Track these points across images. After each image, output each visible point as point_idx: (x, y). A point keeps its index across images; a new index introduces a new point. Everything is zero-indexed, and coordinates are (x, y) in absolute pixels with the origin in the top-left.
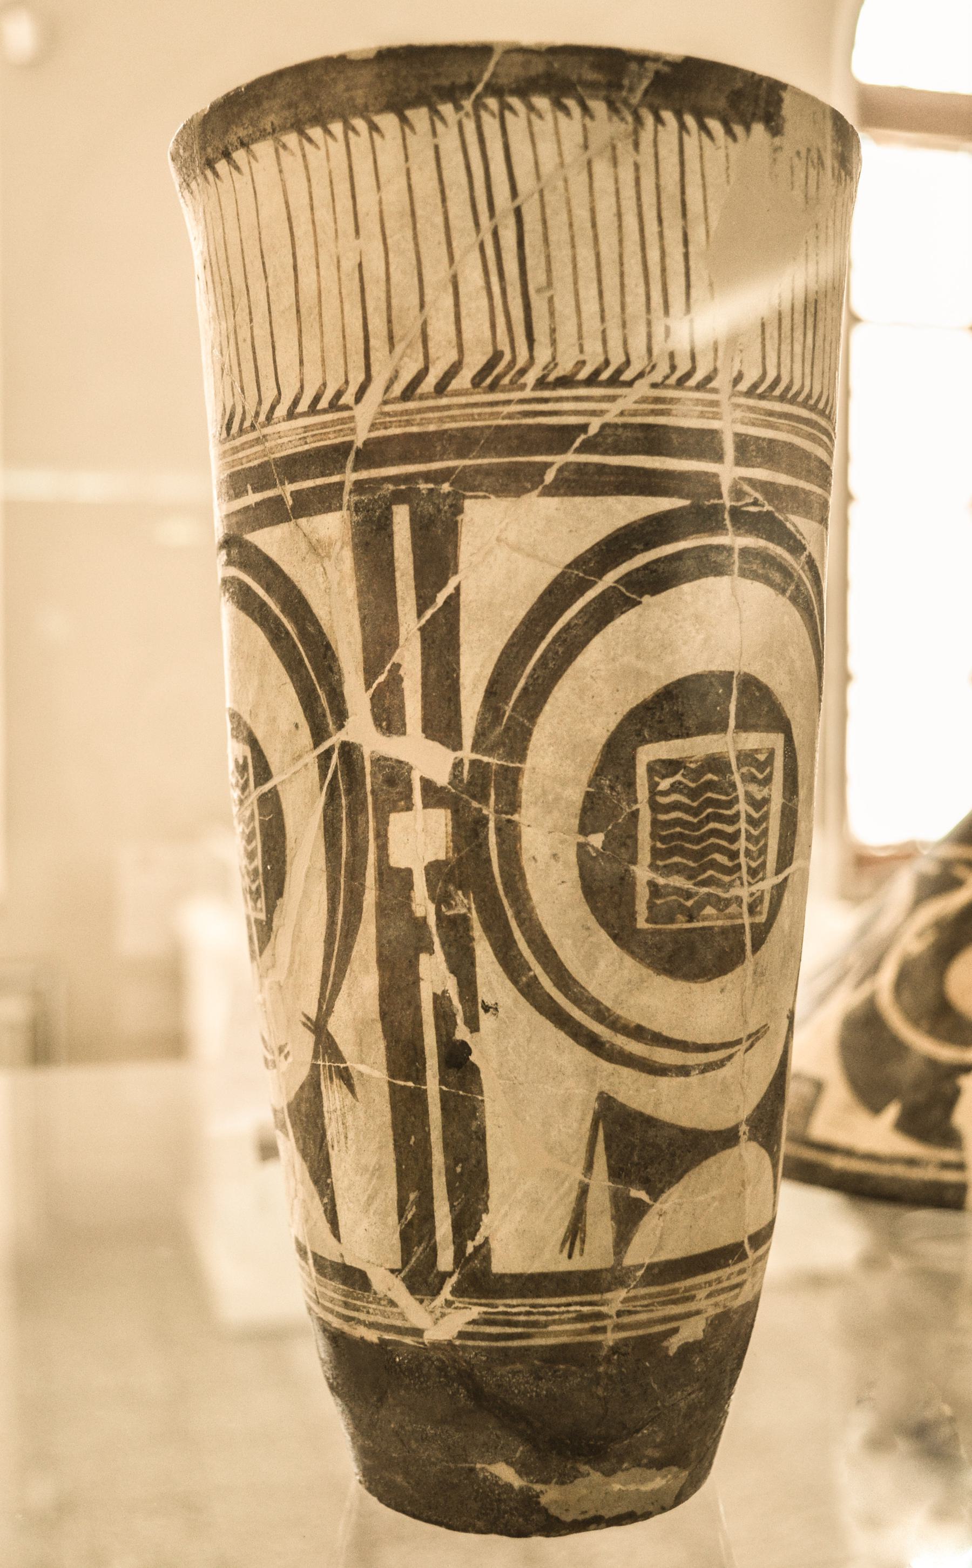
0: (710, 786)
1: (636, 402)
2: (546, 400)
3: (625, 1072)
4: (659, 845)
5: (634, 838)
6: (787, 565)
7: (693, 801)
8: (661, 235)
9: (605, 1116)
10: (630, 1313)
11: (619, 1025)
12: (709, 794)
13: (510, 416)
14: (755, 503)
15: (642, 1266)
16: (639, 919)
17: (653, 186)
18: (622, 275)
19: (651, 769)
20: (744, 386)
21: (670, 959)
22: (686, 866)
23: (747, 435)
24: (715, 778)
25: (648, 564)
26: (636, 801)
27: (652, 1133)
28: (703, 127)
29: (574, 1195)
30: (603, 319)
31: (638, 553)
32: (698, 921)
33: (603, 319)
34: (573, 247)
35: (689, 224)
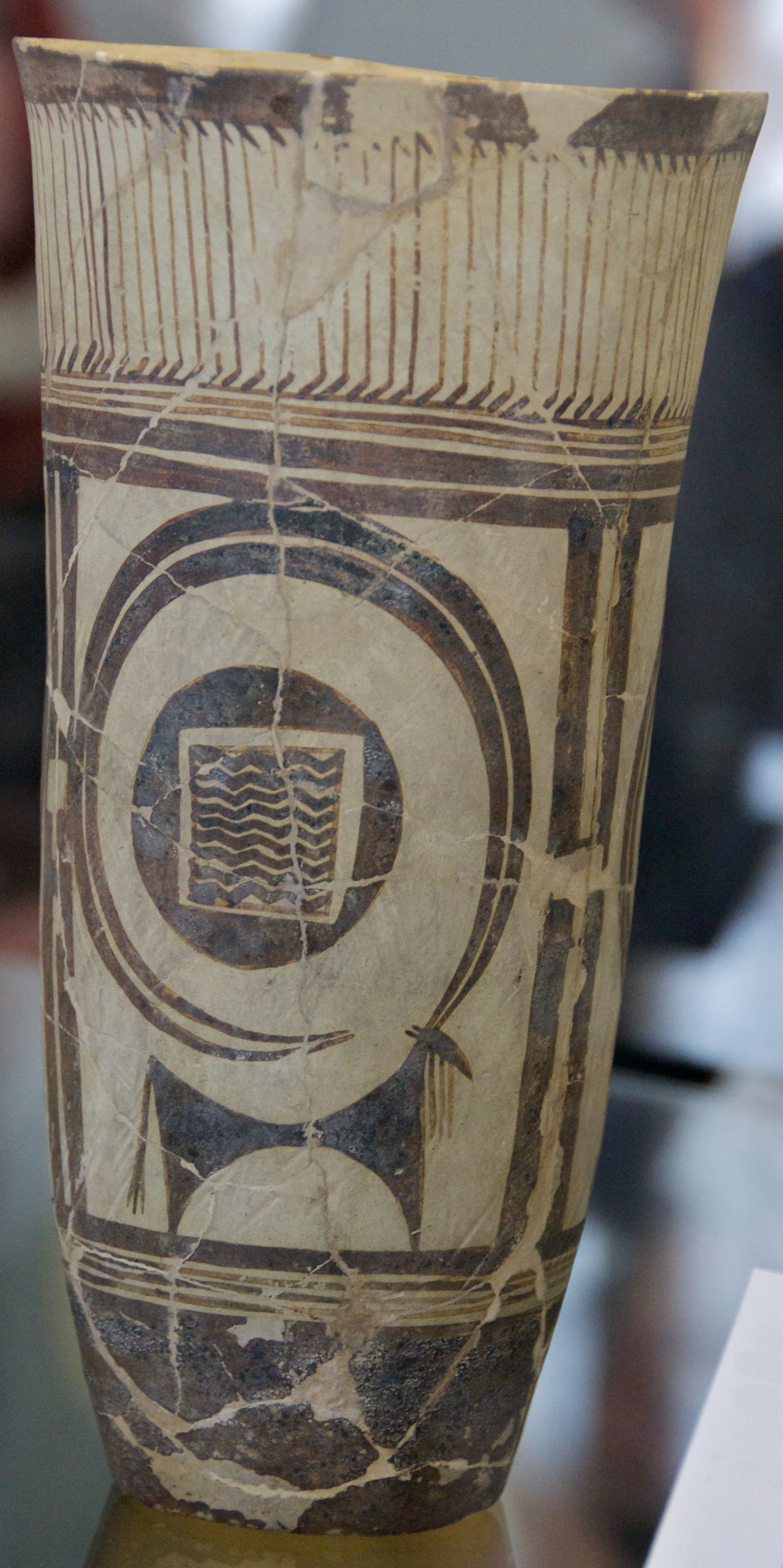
0: (250, 777)
1: (187, 400)
2: (121, 392)
3: (171, 1040)
4: (199, 827)
5: (176, 815)
6: (363, 565)
7: (233, 789)
8: (208, 243)
9: (156, 1080)
10: (188, 1285)
11: (163, 993)
12: (250, 786)
13: (100, 404)
14: (310, 503)
15: (194, 1240)
16: (181, 895)
17: (200, 193)
18: (174, 278)
19: (192, 753)
20: (294, 388)
21: (211, 940)
22: (226, 852)
23: (297, 437)
24: (257, 770)
25: (192, 556)
26: (178, 782)
27: (198, 1107)
28: (245, 135)
29: (134, 1152)
30: (161, 321)
31: (184, 545)
32: (239, 908)
33: (161, 321)
34: (138, 249)
35: (234, 229)
